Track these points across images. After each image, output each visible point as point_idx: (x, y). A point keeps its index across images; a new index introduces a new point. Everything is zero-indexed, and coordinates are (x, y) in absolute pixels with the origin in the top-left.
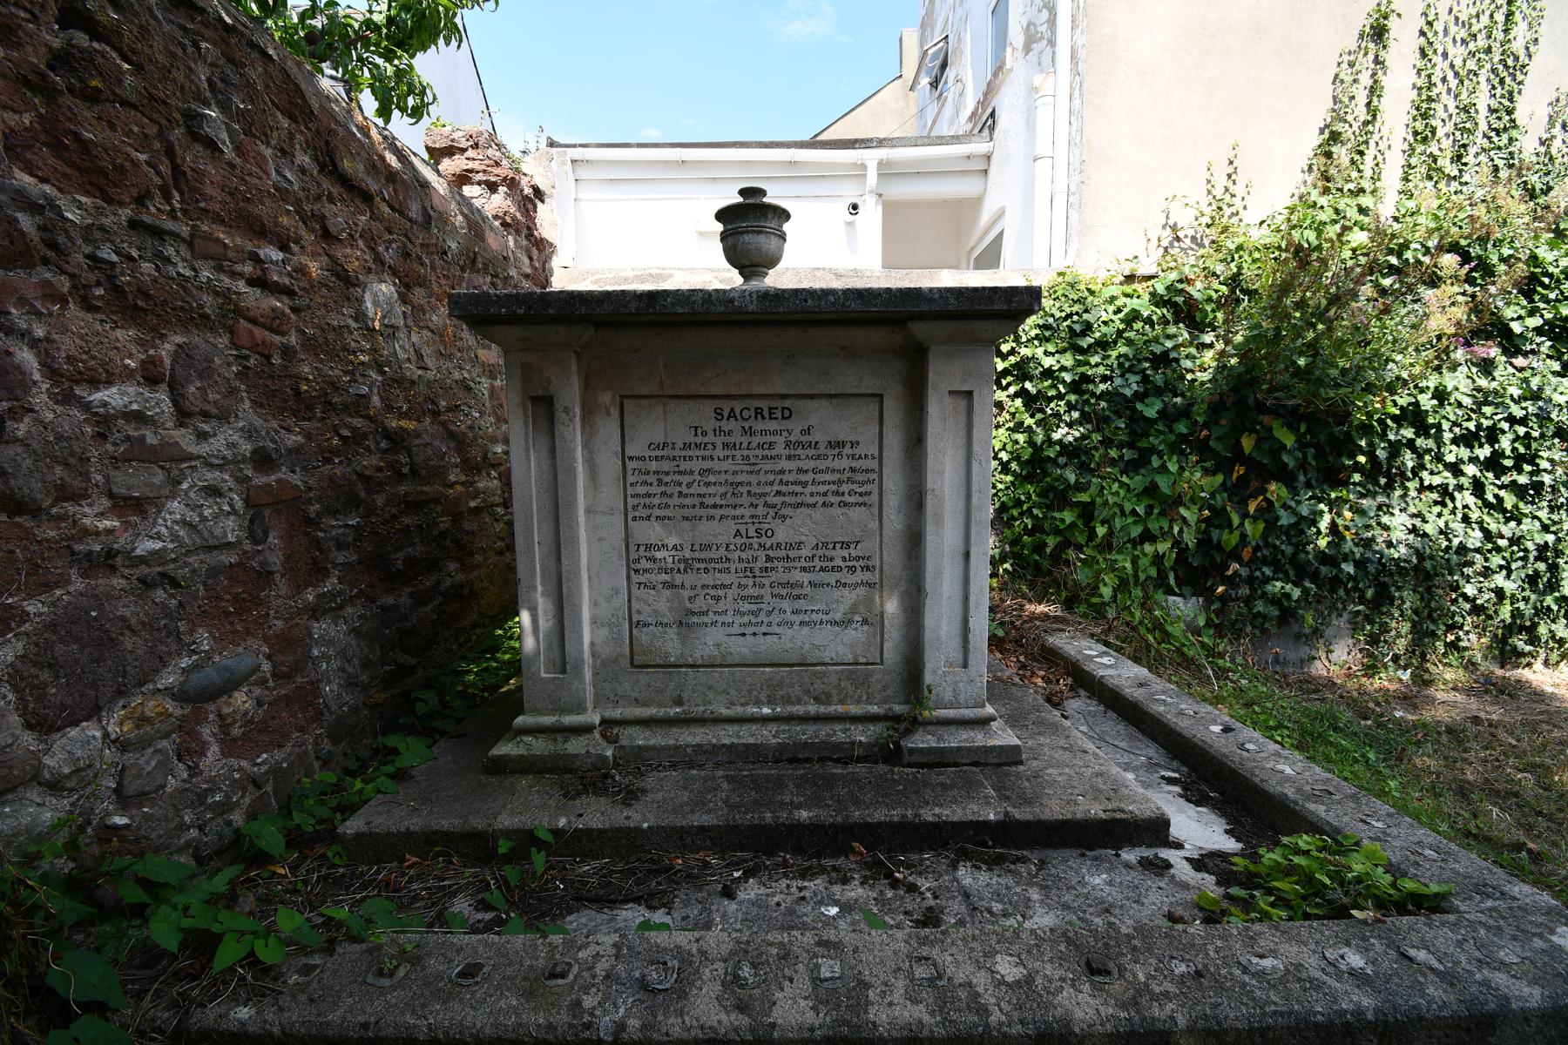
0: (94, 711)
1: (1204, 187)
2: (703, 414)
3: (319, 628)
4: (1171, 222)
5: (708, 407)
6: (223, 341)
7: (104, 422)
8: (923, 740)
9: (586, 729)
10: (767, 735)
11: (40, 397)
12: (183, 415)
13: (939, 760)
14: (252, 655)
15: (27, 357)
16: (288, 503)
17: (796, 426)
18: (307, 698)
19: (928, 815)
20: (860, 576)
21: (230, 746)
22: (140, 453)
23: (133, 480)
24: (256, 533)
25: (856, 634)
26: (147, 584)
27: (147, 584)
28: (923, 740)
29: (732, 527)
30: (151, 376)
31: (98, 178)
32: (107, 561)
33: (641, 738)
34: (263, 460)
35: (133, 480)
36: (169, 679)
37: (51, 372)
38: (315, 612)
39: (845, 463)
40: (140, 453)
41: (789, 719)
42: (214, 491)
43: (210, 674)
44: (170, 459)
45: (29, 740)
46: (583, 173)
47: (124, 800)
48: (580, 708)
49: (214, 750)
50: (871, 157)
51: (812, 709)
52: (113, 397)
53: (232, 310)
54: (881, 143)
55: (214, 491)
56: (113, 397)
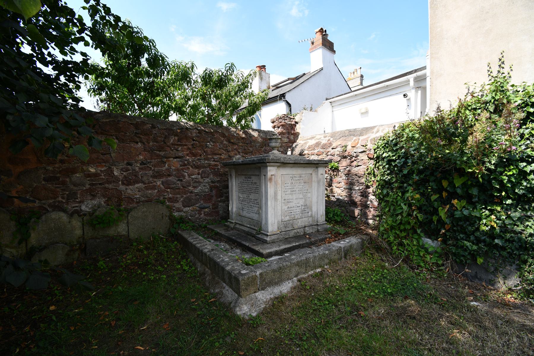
0: (189, 207)
1: (487, 74)
2: (243, 177)
3: (220, 204)
4: (470, 91)
5: (244, 176)
6: (208, 169)
7: (193, 179)
8: (259, 236)
9: (233, 223)
10: (246, 229)
11: (187, 177)
12: (202, 178)
13: (259, 239)
14: (210, 205)
15: (186, 174)
16: (216, 187)
17: (251, 180)
18: (218, 212)
19: (244, 243)
20: (257, 206)
21: (205, 215)
22: (196, 182)
23: (195, 185)
24: (211, 191)
25: (257, 215)
26: (196, 195)
27: (196, 195)
28: (259, 236)
29: (246, 195)
30: (198, 174)
31: (194, 155)
32: (191, 192)
33: (238, 226)
34: (212, 182)
35: (195, 185)
36: (197, 205)
37: (188, 175)
38: (220, 202)
39: (256, 186)
40: (196, 182)
41: (251, 228)
42: (205, 186)
43: (202, 206)
44: (199, 182)
45: (183, 208)
46: (333, 105)
47: (191, 216)
48: (233, 220)
49: (203, 215)
50: (411, 77)
51: (253, 227)
52: (193, 177)
53: (210, 165)
54: (416, 71)
55: (205, 186)
56: (193, 177)
